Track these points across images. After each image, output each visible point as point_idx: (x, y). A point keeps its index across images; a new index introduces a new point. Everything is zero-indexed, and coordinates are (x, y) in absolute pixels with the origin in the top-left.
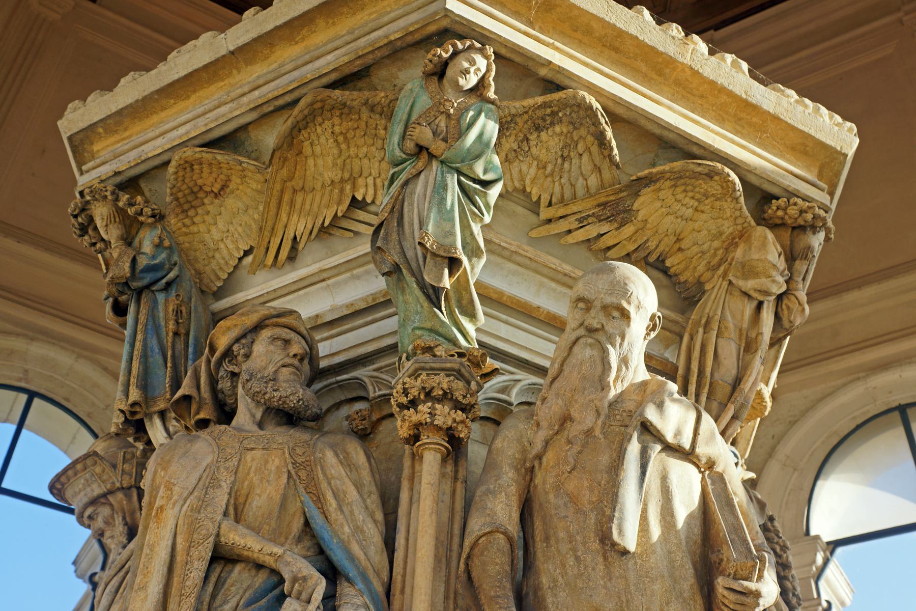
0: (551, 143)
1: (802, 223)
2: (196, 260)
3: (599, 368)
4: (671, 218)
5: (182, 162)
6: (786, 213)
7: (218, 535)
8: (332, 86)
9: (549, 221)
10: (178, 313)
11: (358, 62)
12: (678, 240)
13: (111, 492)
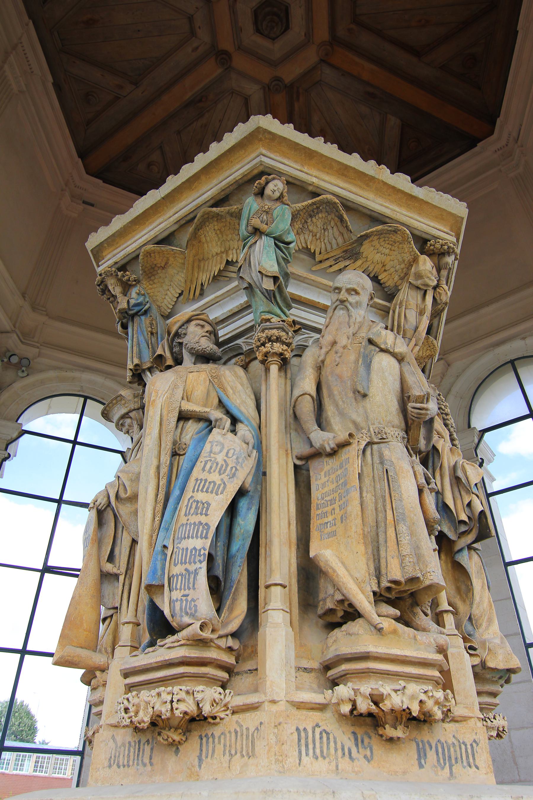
0: (318, 223)
1: (443, 251)
2: (157, 300)
3: (347, 319)
5: (145, 253)
6: (435, 247)
7: (180, 407)
8: (212, 206)
10: (151, 324)
13: (130, 411)
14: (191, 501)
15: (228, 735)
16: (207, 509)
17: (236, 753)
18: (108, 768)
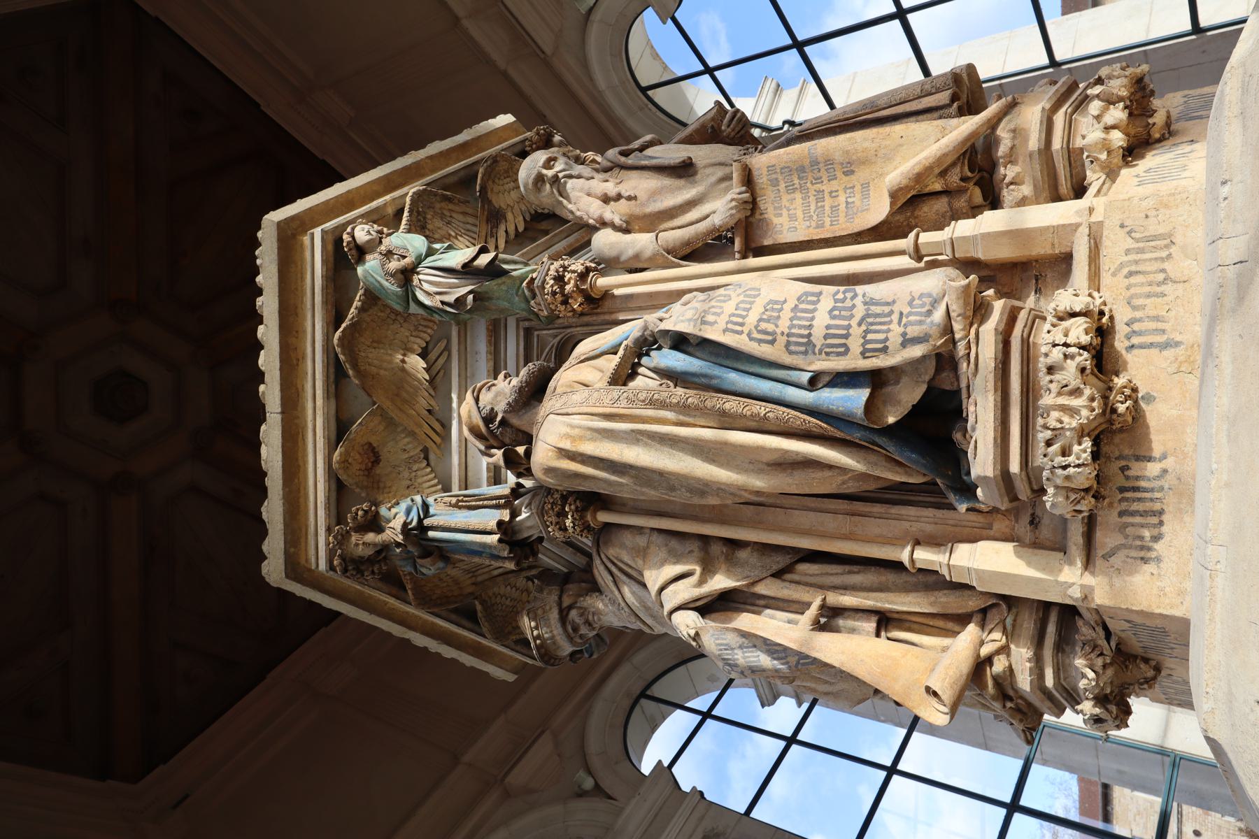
13: (560, 604)
14: (756, 335)
15: (1132, 291)
16: (776, 302)
17: (1163, 271)
18: (1161, 565)
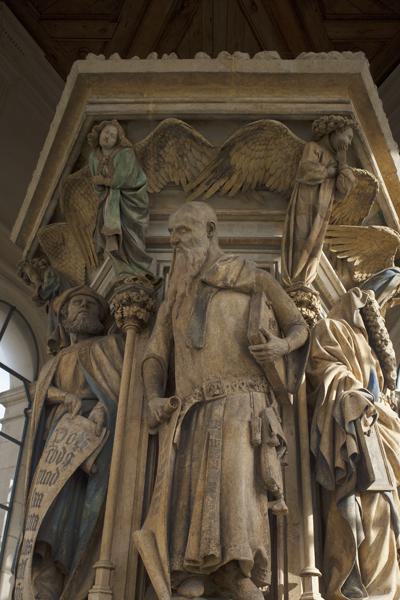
4: (253, 161)
7: (47, 395)
9: (192, 191)
11: (73, 156)
12: (266, 171)
